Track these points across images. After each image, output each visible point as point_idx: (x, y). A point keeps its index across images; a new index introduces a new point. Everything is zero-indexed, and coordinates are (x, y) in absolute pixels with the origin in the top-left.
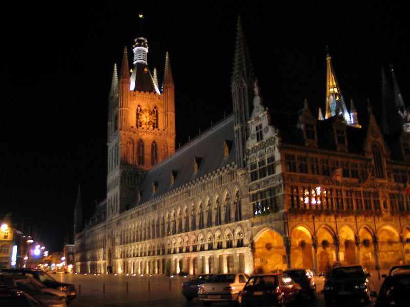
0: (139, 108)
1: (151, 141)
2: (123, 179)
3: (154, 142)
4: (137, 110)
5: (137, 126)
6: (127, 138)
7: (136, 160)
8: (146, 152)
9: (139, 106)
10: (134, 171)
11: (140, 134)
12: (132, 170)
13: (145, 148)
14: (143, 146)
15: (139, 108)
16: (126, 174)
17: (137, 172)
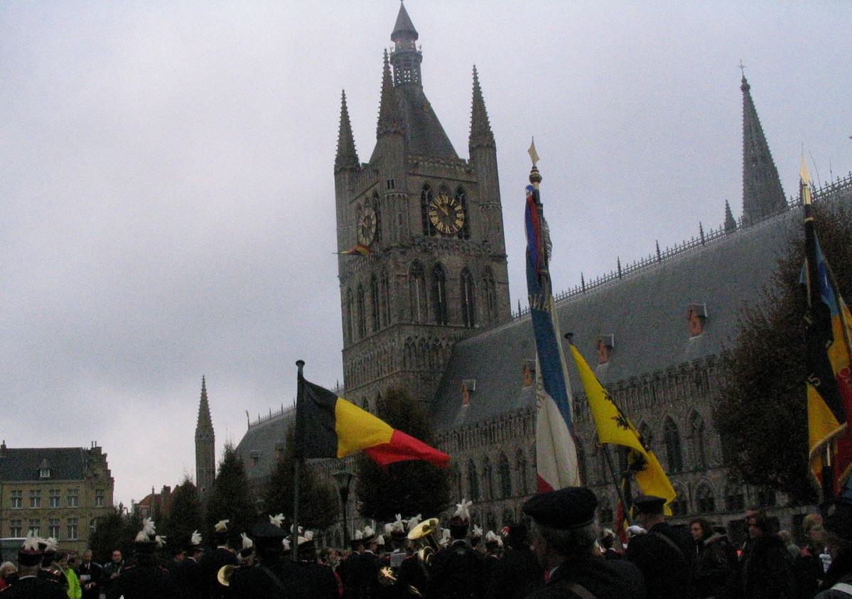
0: (427, 193)
1: (460, 270)
2: (408, 357)
3: (466, 270)
4: (423, 195)
5: (426, 233)
6: (409, 263)
7: (431, 314)
8: (450, 295)
9: (426, 187)
10: (430, 338)
11: (436, 254)
12: (426, 335)
13: (448, 285)
14: (443, 280)
15: (427, 193)
16: (414, 344)
17: (437, 340)
